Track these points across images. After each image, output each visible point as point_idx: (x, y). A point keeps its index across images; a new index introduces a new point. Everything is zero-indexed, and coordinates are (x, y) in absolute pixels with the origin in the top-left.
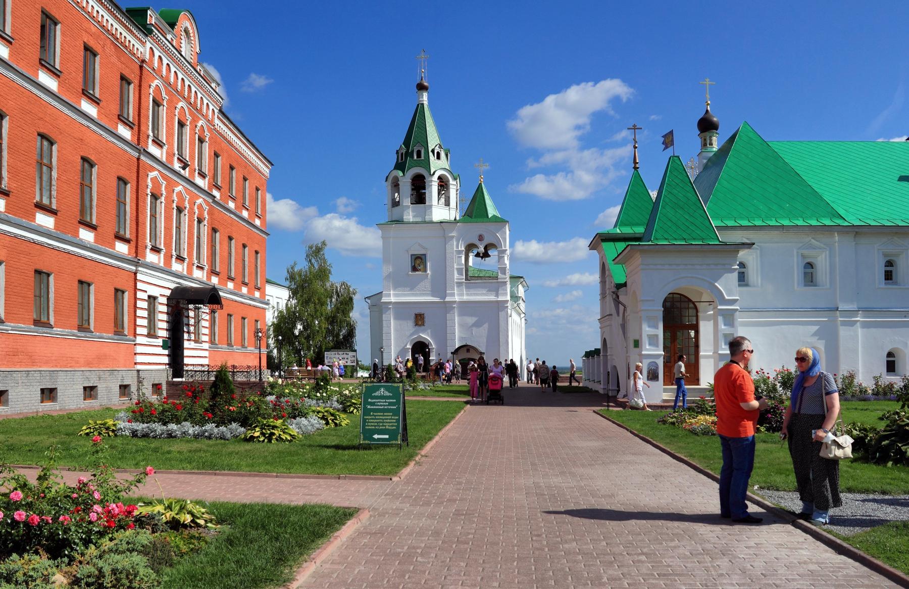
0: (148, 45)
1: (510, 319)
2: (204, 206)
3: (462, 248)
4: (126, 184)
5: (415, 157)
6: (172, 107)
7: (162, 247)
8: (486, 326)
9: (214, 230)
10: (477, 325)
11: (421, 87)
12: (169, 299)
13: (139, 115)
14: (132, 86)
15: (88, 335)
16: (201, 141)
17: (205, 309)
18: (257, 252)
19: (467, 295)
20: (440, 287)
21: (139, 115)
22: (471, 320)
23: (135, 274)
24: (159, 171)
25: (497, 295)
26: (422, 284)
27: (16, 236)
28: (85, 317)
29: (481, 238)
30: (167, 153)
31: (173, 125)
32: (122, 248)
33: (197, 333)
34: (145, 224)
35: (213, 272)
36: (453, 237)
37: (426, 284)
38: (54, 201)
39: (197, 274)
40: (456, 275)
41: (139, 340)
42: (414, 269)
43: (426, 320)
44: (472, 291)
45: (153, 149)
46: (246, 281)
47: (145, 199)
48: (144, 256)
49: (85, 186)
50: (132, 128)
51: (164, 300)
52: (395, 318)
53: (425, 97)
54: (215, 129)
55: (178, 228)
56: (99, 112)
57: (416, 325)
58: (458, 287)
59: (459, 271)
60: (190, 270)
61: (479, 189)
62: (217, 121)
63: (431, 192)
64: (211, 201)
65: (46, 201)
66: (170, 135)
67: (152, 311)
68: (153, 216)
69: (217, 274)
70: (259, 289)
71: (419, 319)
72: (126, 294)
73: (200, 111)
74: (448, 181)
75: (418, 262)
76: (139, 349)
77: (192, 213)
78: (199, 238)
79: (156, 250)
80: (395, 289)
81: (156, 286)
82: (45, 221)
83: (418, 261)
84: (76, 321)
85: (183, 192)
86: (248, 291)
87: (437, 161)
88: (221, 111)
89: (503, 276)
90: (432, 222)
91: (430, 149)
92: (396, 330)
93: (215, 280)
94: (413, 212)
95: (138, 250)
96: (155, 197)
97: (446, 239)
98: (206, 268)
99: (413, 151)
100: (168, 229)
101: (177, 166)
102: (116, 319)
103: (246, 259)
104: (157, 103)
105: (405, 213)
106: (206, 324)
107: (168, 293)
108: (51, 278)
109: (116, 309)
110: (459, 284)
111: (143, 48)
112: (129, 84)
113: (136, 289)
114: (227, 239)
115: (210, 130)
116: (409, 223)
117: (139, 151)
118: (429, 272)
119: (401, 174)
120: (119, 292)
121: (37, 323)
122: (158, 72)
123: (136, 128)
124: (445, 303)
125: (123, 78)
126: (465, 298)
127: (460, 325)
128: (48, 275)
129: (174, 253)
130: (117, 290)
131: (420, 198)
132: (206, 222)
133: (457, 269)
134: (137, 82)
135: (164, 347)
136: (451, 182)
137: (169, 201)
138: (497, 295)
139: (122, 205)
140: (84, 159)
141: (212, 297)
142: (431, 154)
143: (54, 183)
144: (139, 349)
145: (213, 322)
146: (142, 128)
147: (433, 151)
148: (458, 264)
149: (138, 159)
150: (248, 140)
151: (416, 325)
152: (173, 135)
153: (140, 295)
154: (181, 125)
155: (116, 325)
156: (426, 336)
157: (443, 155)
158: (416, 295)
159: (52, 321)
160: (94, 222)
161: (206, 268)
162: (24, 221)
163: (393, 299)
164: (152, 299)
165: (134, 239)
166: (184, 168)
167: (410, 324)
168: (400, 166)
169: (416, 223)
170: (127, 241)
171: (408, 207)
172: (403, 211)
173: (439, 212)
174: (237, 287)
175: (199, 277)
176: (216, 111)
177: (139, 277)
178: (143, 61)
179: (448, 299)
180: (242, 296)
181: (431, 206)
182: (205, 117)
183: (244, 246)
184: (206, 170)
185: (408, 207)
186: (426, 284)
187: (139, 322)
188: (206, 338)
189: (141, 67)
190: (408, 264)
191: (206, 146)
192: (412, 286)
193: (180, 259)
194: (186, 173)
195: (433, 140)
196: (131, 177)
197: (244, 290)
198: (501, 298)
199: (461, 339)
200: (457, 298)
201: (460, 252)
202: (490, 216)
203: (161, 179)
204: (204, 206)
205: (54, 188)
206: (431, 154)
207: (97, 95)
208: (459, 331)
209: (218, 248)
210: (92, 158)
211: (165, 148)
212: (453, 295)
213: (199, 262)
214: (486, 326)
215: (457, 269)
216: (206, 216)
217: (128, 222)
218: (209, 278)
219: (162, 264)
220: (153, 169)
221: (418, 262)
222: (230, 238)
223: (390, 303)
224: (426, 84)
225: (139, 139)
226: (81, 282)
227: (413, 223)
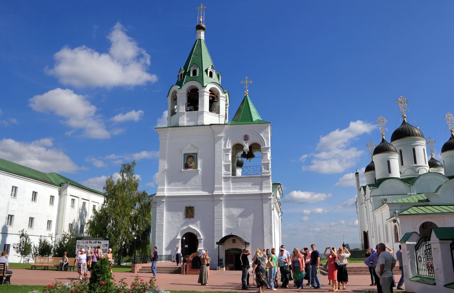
1: (273, 211)
3: (229, 146)
5: (191, 75)
8: (251, 217)
11: (199, 28)
19: (234, 189)
20: (209, 182)
26: (193, 180)
29: (246, 138)
36: (221, 137)
37: (197, 179)
40: (224, 171)
42: (187, 166)
43: (196, 212)
44: (238, 185)
52: (169, 210)
53: (202, 35)
58: (225, 181)
61: (245, 101)
63: (203, 101)
71: (189, 212)
74: (219, 94)
75: (190, 160)
83: (190, 160)
87: (210, 79)
89: (267, 171)
91: (204, 69)
92: (169, 222)
94: (187, 117)
97: (215, 140)
99: (189, 71)
105: (181, 118)
118: (199, 168)
124: (213, 196)
126: (232, 192)
127: (228, 217)
131: (193, 102)
133: (225, 165)
136: (221, 94)
142: (204, 73)
147: (206, 71)
148: (226, 161)
156: (195, 228)
157: (214, 74)
158: (187, 190)
163: (166, 193)
167: (182, 214)
171: (183, 114)
173: (209, 118)
179: (216, 193)
181: (202, 113)
185: (183, 114)
186: (197, 179)
190: (181, 161)
195: (207, 62)
198: (264, 191)
199: (227, 230)
200: (224, 192)
201: (227, 151)
202: (254, 120)
206: (204, 73)
208: (226, 223)
212: (221, 189)
214: (251, 217)
215: (225, 165)
221: (190, 160)
223: (163, 197)
224: (204, 26)
227: (186, 126)
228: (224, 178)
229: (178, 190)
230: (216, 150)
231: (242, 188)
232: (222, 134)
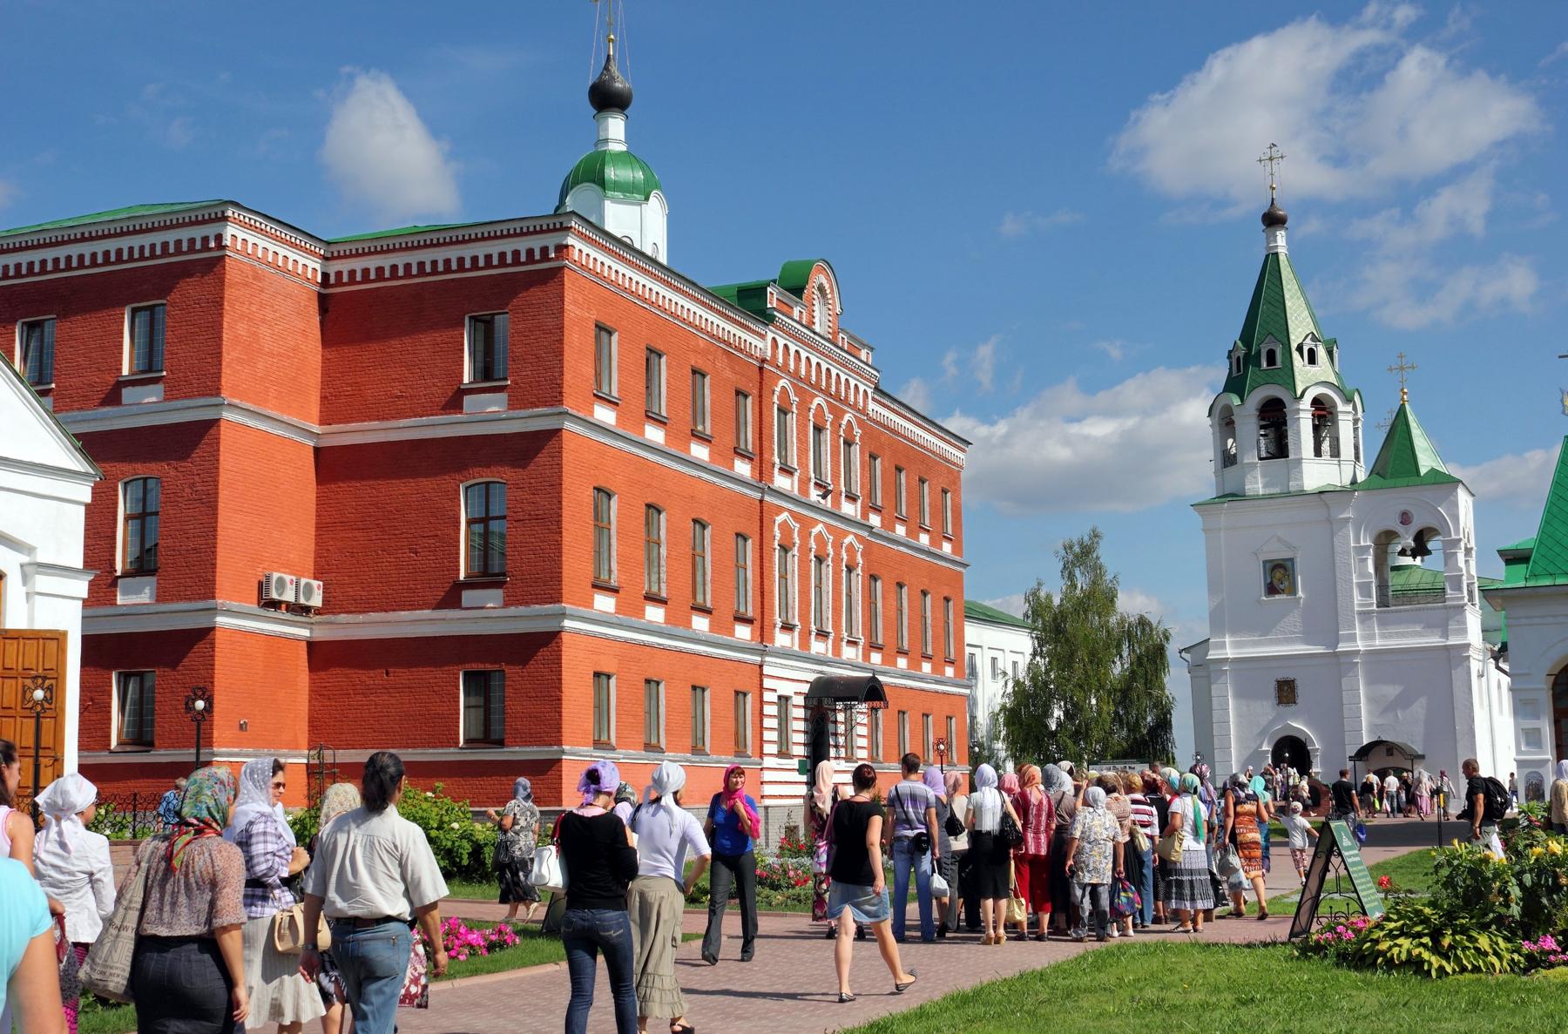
0: (770, 336)
2: (857, 545)
4: (745, 540)
6: (804, 407)
7: (797, 622)
9: (874, 578)
10: (1403, 702)
12: (807, 697)
13: (761, 438)
14: (750, 400)
15: (704, 758)
16: (848, 444)
17: (863, 707)
18: (947, 600)
19: (1383, 636)
21: (761, 438)
22: (1392, 691)
23: (761, 666)
24: (790, 511)
25: (1445, 635)
27: (626, 641)
28: (699, 735)
30: (800, 480)
31: (806, 435)
32: (743, 632)
34: (772, 592)
35: (873, 646)
37: (1294, 619)
38: (663, 586)
39: (849, 653)
40: (1357, 598)
41: (769, 762)
42: (1272, 590)
45: (781, 482)
46: (930, 652)
47: (772, 557)
48: (772, 640)
49: (696, 558)
50: (751, 459)
51: (800, 700)
54: (870, 419)
55: (819, 587)
56: (711, 454)
57: (1280, 702)
58: (1362, 622)
59: (1364, 589)
60: (837, 650)
62: (872, 406)
64: (865, 534)
65: (655, 589)
66: (803, 452)
67: (783, 718)
68: (784, 577)
69: (879, 648)
70: (952, 663)
71: (1286, 692)
72: (749, 697)
73: (845, 402)
75: (1278, 577)
76: (767, 776)
77: (837, 560)
78: (849, 596)
79: (787, 627)
80: (1233, 633)
81: (789, 681)
82: (655, 614)
83: (1278, 574)
84: (689, 742)
85: (825, 532)
86: (934, 670)
88: (877, 389)
90: (1302, 493)
92: (1239, 715)
93: (876, 658)
95: (763, 634)
96: (785, 549)
97: (1333, 525)
98: (862, 642)
100: (804, 593)
101: (814, 495)
102: (737, 734)
103: (929, 614)
104: (783, 411)
106: (862, 730)
107: (805, 688)
108: (662, 687)
109: (737, 720)
110: (1365, 616)
111: (759, 342)
112: (746, 397)
114: (894, 588)
115: (861, 423)
116: (1257, 498)
117: (762, 491)
118: (1300, 594)
119: (1236, 401)
120: (740, 694)
121: (648, 747)
122: (784, 368)
123: (757, 459)
124: (1336, 655)
125: (738, 393)
126: (1379, 643)
127: (1370, 700)
128: (658, 683)
129: (813, 628)
130: (737, 693)
132: (859, 570)
134: (756, 392)
135: (800, 771)
137: (804, 549)
138: (1445, 635)
139: (741, 571)
140: (695, 521)
141: (872, 692)
143: (663, 562)
144: (767, 776)
146: (766, 456)
149: (761, 501)
150: (924, 418)
151: (1280, 702)
152: (807, 451)
153: (768, 696)
154: (818, 429)
155: (737, 743)
156: (1299, 726)
158: (1278, 642)
159: (663, 744)
160: (709, 605)
161: (862, 642)
162: (634, 621)
163: (1230, 653)
164: (783, 700)
165: (758, 617)
166: (824, 497)
168: (1235, 384)
169: (1271, 497)
170: (749, 621)
172: (1244, 477)
173: (1317, 473)
174: (915, 665)
175: (851, 662)
176: (870, 391)
177: (766, 670)
178: (763, 361)
179: (1343, 647)
180: (921, 679)
182: (854, 407)
183: (924, 593)
184: (857, 489)
186: (1294, 619)
187: (768, 735)
189: (761, 369)
190: (1258, 580)
191: (856, 450)
192: (1263, 628)
193: (822, 634)
194: (828, 503)
196: (752, 529)
197: (927, 667)
199: (1373, 727)
200: (1361, 645)
203: (792, 523)
204: (857, 545)
205: (663, 569)
207: (708, 432)
208: (1370, 712)
209: (879, 605)
210: (705, 517)
211: (797, 474)
212: (1352, 638)
213: (850, 635)
216: (860, 560)
217: (750, 593)
218: (866, 657)
219: (796, 648)
220: (780, 510)
221: (1278, 577)
222: (900, 585)
225: (761, 473)
226: (694, 688)
228: (1360, 613)
229: (1255, 644)
230: (1338, 549)
231: (1403, 635)
232: (1349, 514)
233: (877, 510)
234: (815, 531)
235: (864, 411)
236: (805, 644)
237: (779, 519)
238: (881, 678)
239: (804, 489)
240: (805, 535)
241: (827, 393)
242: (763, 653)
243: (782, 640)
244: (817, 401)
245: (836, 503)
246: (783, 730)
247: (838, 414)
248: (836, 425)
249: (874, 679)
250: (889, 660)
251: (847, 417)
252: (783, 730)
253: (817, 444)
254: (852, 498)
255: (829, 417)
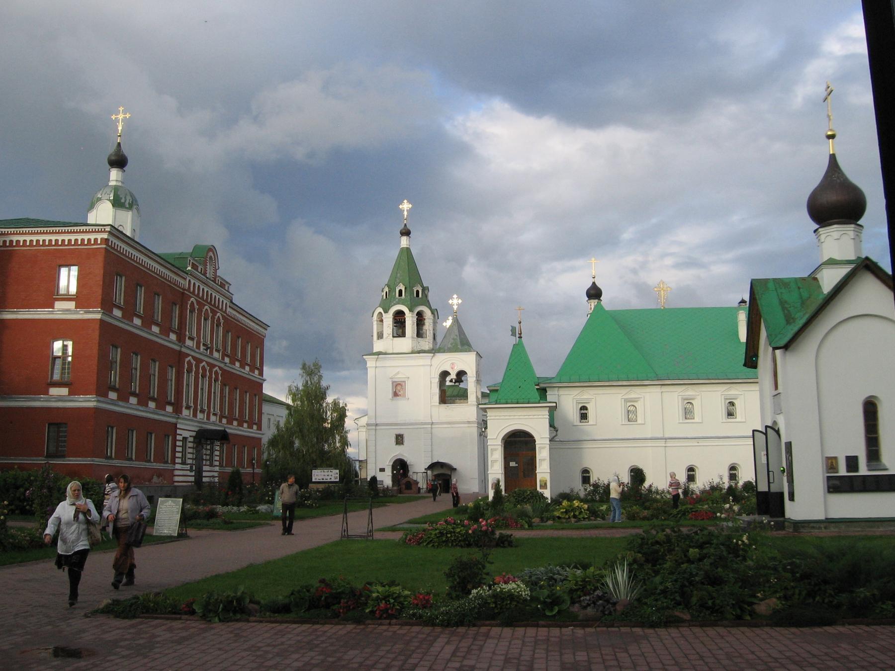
0: (188, 279)
17: (219, 443)
32: (169, 409)
33: (211, 460)
39: (213, 418)
41: (178, 466)
51: (191, 439)
62: (229, 309)
66: (199, 330)
67: (184, 447)
69: (225, 417)
76: (176, 473)
77: (210, 377)
79: (188, 408)
81: (187, 429)
106: (217, 453)
107: (194, 434)
113: (175, 434)
135: (191, 470)
137: (197, 373)
141: (223, 436)
144: (176, 473)
145: (221, 451)
153: (179, 438)
164: (185, 439)
175: (214, 423)
177: (178, 426)
188: (217, 463)
193: (202, 411)
203: (192, 361)
218: (220, 421)
222: (236, 389)
233: (228, 356)
234: (201, 365)
235: (225, 312)
236: (195, 415)
237: (187, 360)
238: (228, 430)
239: (198, 347)
240: (197, 367)
241: (210, 303)
242: (178, 418)
243: (185, 412)
244: (206, 307)
245: (211, 353)
246: (184, 452)
247: (214, 313)
248: (213, 318)
249: (225, 431)
250: (230, 422)
251: (218, 314)
252: (184, 452)
253: (205, 324)
254: (218, 351)
255: (211, 315)
